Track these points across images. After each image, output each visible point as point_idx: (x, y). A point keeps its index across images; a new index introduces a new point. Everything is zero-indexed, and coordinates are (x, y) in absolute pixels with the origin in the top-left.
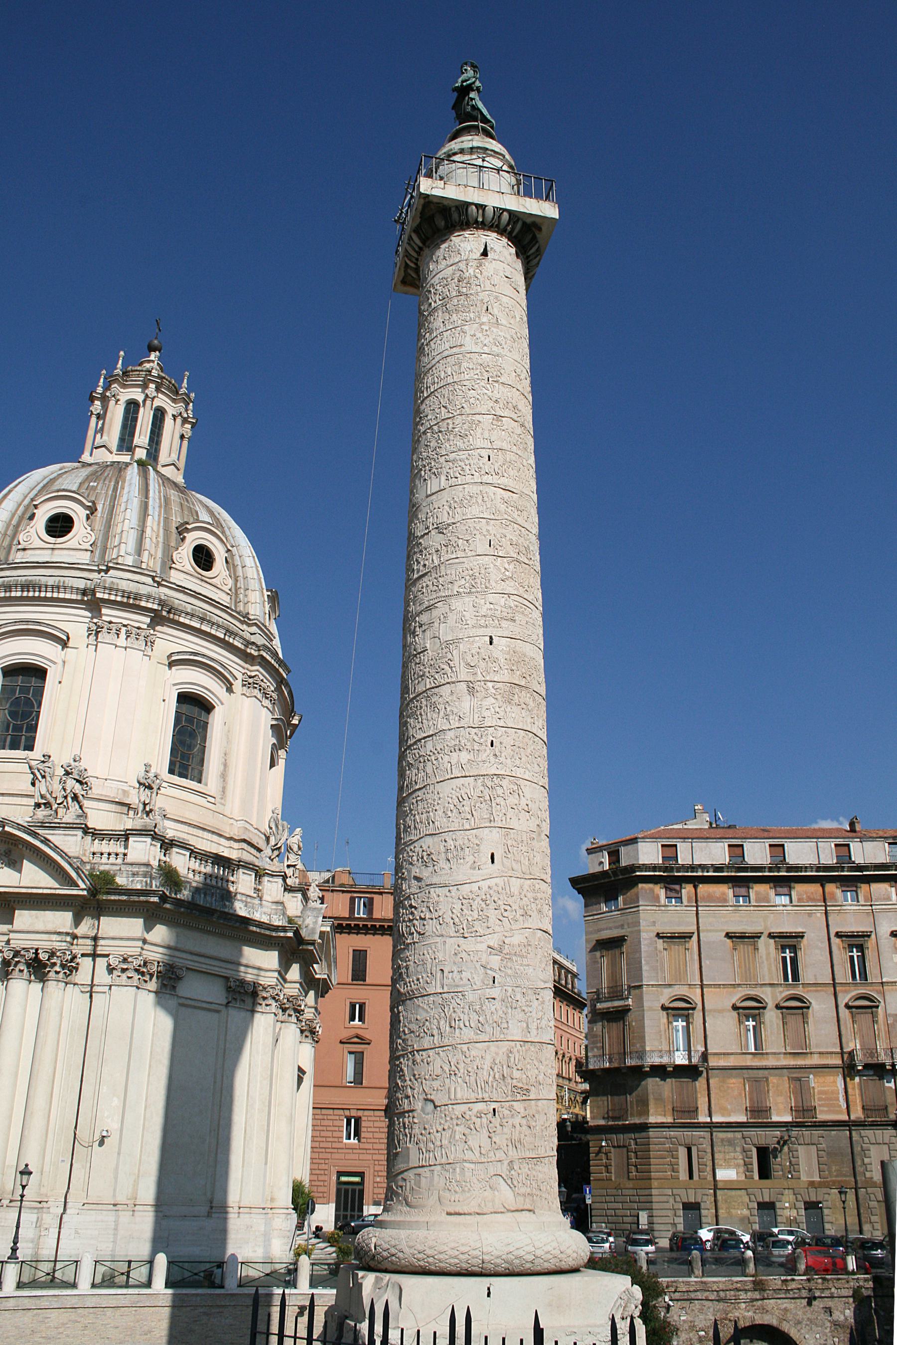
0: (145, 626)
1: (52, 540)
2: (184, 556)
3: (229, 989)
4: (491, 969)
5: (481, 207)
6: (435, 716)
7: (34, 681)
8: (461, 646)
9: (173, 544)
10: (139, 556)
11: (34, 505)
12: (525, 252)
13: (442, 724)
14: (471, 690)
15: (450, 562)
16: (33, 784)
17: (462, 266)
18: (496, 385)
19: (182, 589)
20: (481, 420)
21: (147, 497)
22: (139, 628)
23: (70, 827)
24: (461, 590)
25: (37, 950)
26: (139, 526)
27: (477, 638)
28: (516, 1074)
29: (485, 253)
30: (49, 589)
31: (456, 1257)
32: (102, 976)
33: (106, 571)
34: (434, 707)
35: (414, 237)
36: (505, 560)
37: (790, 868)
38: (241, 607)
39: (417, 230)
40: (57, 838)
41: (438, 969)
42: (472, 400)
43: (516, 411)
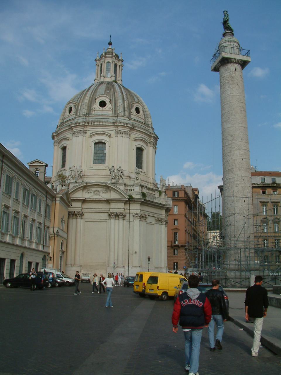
0: (128, 131)
1: (101, 108)
2: (134, 111)
3: (156, 220)
5: (235, 59)
7: (103, 146)
9: (131, 107)
10: (124, 112)
13: (234, 176)
16: (110, 173)
19: (135, 120)
21: (123, 95)
22: (127, 132)
23: (121, 184)
25: (117, 212)
29: (236, 70)
32: (132, 218)
33: (118, 117)
34: (232, 172)
35: (219, 63)
37: (277, 185)
38: (146, 123)
39: (220, 62)
40: (118, 186)
42: (236, 107)
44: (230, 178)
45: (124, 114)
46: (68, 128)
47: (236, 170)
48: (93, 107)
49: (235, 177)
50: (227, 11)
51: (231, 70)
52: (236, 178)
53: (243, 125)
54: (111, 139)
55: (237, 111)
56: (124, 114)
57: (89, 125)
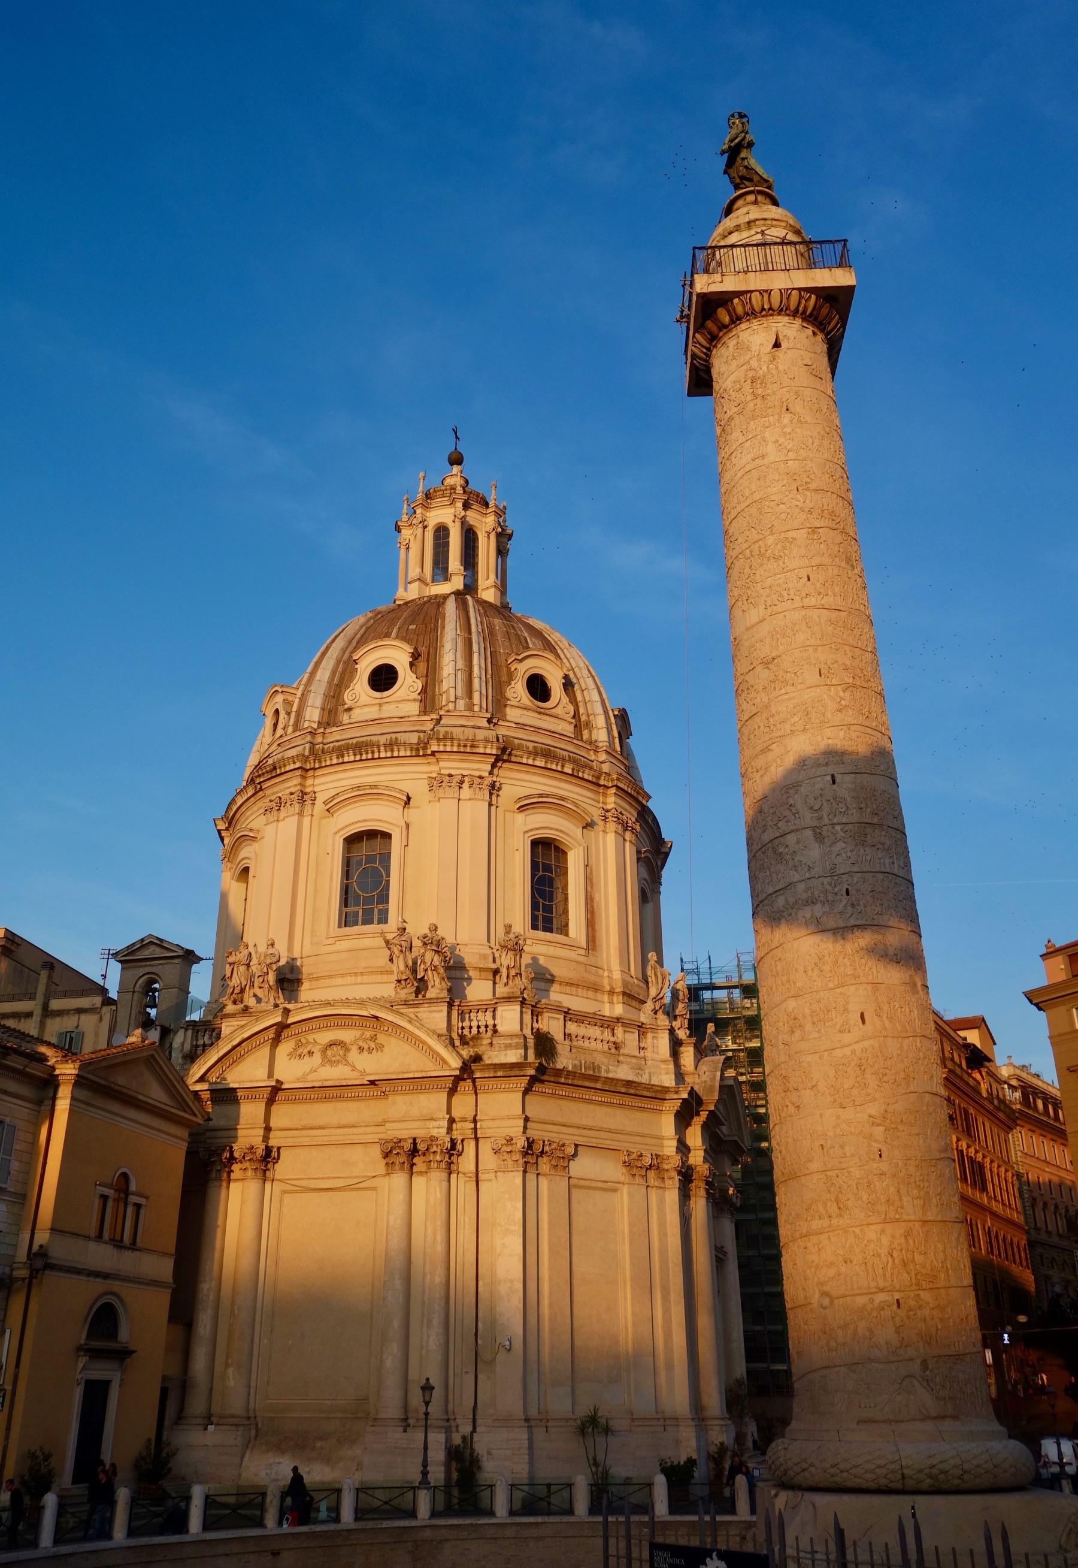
1: (378, 694)
4: (875, 1141)
5: (769, 292)
6: (782, 868)
8: (802, 789)
11: (355, 661)
12: (824, 328)
14: (819, 837)
15: (779, 698)
17: (754, 363)
18: (808, 493)
20: (795, 536)
24: (794, 728)
26: (466, 666)
27: (819, 779)
28: (919, 1258)
30: (382, 749)
31: (872, 1472)
34: (780, 857)
36: (839, 688)
41: (817, 1144)
43: (834, 518)
44: (771, 890)
45: (470, 707)
46: (251, 791)
47: (798, 842)
48: (347, 697)
49: (797, 877)
50: (745, 112)
51: (755, 348)
52: (801, 886)
53: (829, 601)
54: (412, 814)
55: (790, 534)
56: (470, 707)
57: (319, 768)
